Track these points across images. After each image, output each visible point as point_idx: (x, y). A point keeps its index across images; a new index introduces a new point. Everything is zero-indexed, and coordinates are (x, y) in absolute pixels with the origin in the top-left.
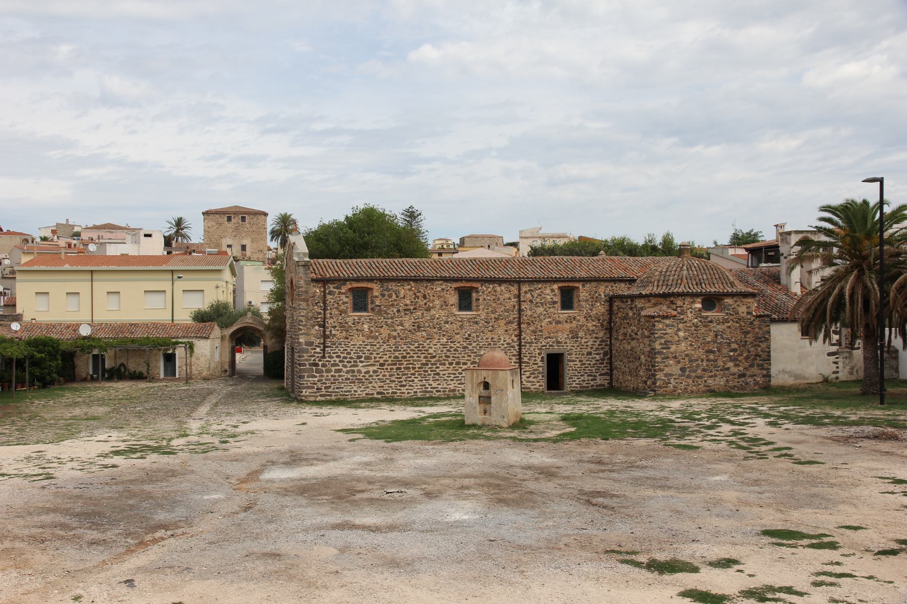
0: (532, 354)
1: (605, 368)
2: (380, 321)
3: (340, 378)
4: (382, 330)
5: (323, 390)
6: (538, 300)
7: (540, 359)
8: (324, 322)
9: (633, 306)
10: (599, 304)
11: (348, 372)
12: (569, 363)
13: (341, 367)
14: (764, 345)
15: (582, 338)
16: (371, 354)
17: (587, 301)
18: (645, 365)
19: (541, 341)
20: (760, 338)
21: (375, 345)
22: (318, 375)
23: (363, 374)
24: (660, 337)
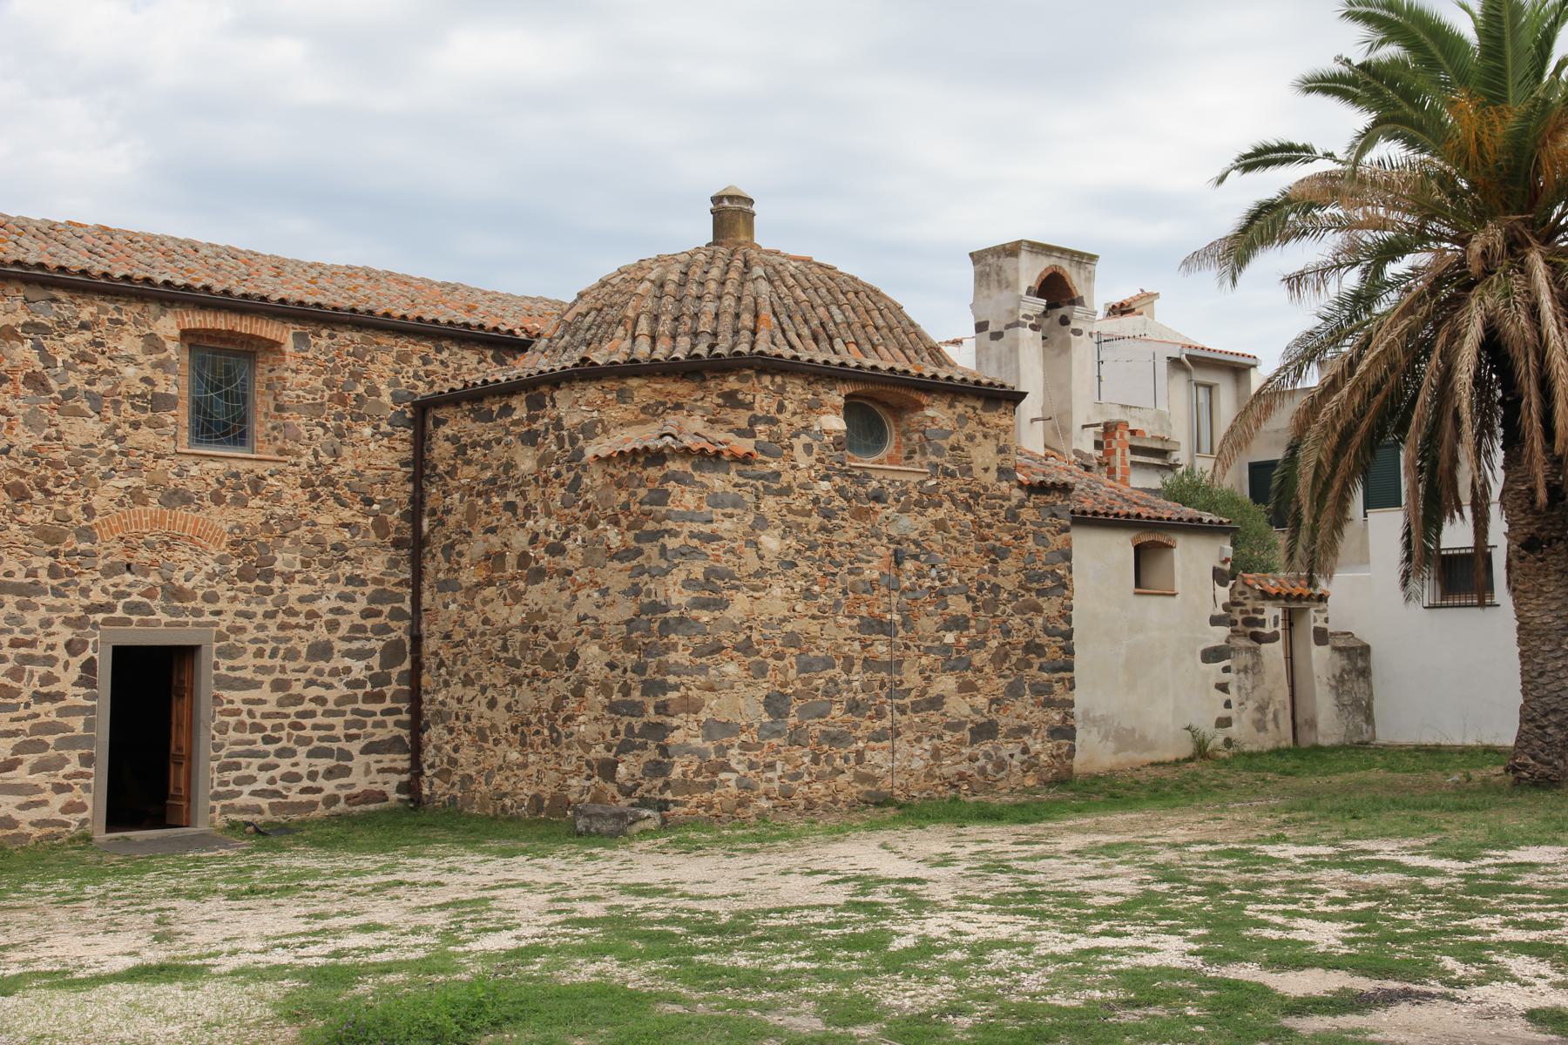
0: (32, 644)
1: (390, 720)
6: (75, 380)
7: (75, 672)
9: (538, 426)
10: (368, 431)
12: (226, 694)
14: (1051, 606)
15: (288, 578)
17: (316, 409)
18: (605, 688)
19: (84, 581)
20: (1040, 578)
24: (687, 553)
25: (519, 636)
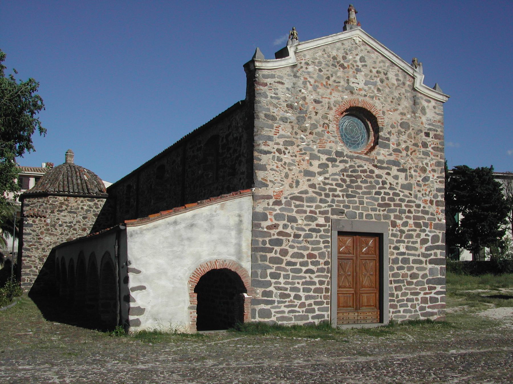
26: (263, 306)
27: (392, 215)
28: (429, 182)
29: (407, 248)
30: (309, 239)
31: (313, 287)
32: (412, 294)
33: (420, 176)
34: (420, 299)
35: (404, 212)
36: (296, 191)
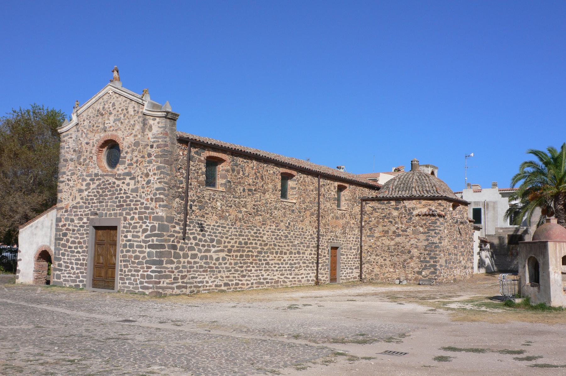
2: (230, 199)
3: (195, 266)
4: (231, 210)
5: (180, 280)
8: (186, 193)
11: (202, 258)
13: (196, 252)
16: (222, 237)
21: (225, 227)
22: (175, 260)
23: (214, 261)
25: (393, 247)
26: (58, 272)
27: (124, 213)
28: (151, 184)
29: (133, 236)
30: (79, 232)
31: (79, 262)
32: (135, 271)
33: (144, 181)
34: (140, 275)
35: (132, 209)
36: (74, 203)
